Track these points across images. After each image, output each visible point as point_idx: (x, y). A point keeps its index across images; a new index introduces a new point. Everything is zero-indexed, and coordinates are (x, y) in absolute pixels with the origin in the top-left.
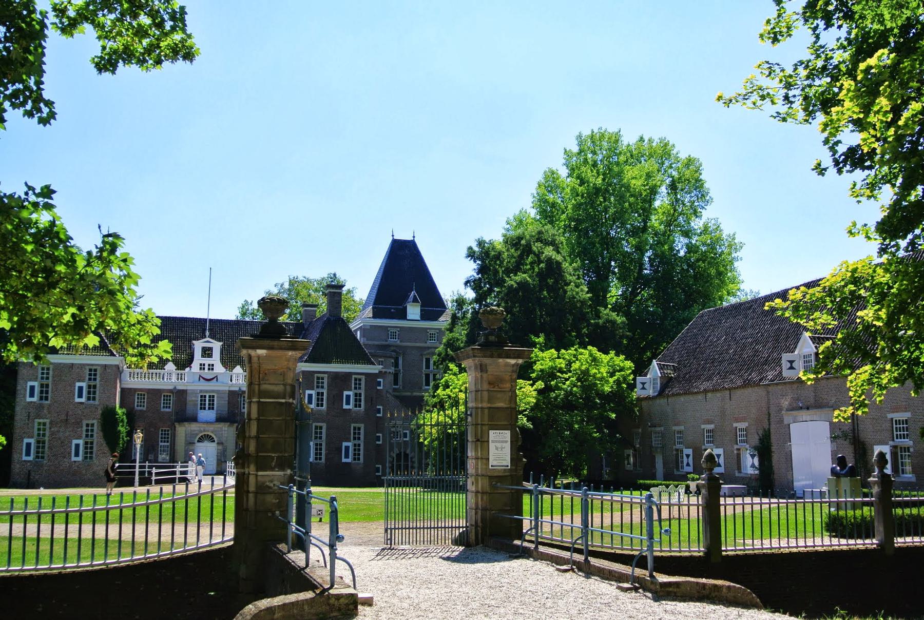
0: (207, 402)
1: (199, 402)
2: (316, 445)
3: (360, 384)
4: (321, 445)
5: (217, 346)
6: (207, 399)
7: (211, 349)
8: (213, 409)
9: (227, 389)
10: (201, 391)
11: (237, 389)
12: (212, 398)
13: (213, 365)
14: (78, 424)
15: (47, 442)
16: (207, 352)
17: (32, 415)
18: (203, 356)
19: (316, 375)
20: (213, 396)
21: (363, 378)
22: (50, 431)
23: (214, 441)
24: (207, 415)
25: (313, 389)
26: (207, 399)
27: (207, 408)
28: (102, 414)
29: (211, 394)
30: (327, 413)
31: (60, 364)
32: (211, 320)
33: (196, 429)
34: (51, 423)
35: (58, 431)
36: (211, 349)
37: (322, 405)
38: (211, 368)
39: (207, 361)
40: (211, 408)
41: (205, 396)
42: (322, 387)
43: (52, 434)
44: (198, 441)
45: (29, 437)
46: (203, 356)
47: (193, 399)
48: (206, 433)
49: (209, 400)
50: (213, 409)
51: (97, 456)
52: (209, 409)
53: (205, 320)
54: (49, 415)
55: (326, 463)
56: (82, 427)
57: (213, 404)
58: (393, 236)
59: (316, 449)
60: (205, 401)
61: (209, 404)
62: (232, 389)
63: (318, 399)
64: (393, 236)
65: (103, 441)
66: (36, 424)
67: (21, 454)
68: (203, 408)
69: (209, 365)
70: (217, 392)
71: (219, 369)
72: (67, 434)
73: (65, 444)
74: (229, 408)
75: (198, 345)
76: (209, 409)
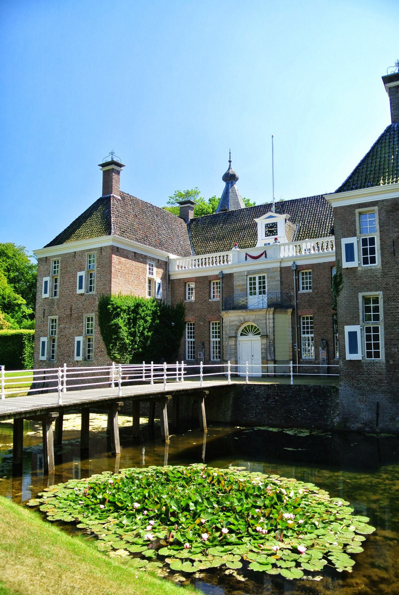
0: (257, 286)
1: (249, 287)
2: (368, 330)
4: (376, 330)
6: (257, 281)
7: (275, 225)
9: (277, 265)
10: (249, 273)
11: (290, 264)
14: (80, 318)
15: (56, 340)
16: (271, 230)
17: (46, 311)
18: (267, 235)
19: (357, 211)
20: (264, 277)
22: (59, 328)
25: (355, 235)
26: (257, 281)
27: (257, 294)
28: (100, 303)
29: (262, 275)
30: (384, 274)
31: (66, 254)
33: (232, 319)
34: (59, 319)
35: (64, 328)
36: (275, 225)
37: (373, 261)
41: (254, 278)
43: (60, 331)
44: (242, 335)
45: (44, 336)
46: (267, 235)
47: (241, 283)
48: (246, 325)
49: (260, 283)
50: (264, 293)
51: (96, 355)
52: (260, 293)
54: (58, 311)
55: (387, 361)
56: (83, 322)
57: (264, 287)
59: (368, 338)
60: (255, 284)
61: (260, 288)
62: (284, 265)
63: (365, 252)
65: (100, 338)
66: (49, 322)
67: (39, 354)
70: (267, 270)
72: (71, 331)
73: (70, 341)
74: (282, 290)
76: (260, 293)
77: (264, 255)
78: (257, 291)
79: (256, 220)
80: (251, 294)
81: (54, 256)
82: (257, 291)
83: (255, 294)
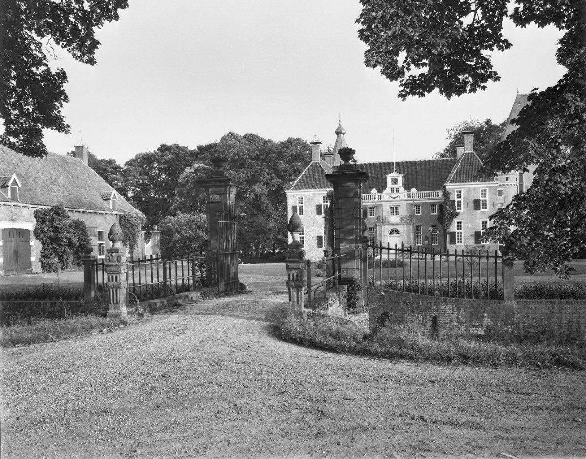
3: (486, 194)
5: (400, 178)
6: (395, 209)
8: (398, 214)
12: (397, 208)
13: (398, 189)
16: (395, 181)
18: (392, 184)
21: (488, 189)
23: (399, 234)
24: (395, 219)
26: (395, 209)
32: (396, 163)
38: (398, 190)
39: (395, 186)
40: (397, 214)
42: (460, 197)
44: (390, 234)
46: (392, 184)
49: (396, 210)
50: (398, 214)
52: (396, 214)
53: (393, 163)
57: (398, 212)
58: (518, 92)
64: (518, 92)
68: (392, 214)
69: (396, 189)
71: (402, 189)
75: (389, 177)
76: (396, 214)
77: (398, 197)
78: (395, 213)
79: (387, 176)
80: (391, 215)
81: (299, 195)
82: (395, 213)
83: (393, 215)
